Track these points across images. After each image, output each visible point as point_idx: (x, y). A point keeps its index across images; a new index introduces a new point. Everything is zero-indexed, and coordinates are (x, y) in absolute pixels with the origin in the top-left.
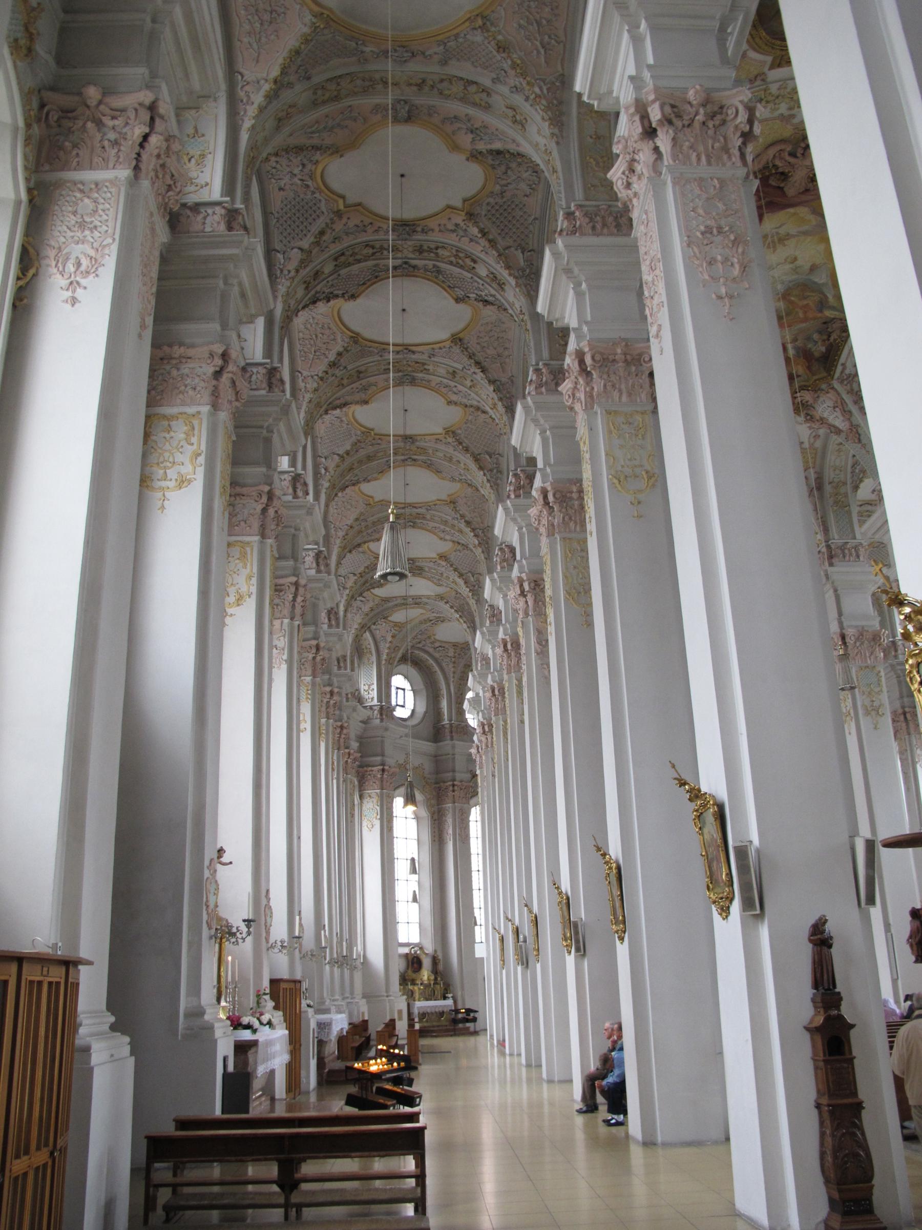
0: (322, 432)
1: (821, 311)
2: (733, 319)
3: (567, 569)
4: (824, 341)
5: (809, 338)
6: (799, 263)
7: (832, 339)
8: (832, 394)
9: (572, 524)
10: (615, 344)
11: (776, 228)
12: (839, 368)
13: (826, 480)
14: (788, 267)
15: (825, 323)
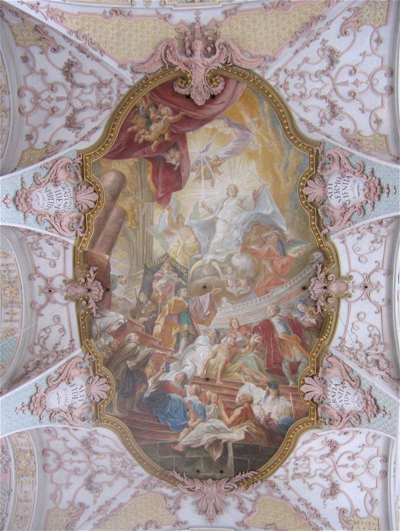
1: (284, 254)
5: (293, 308)
7: (319, 308)
11: (204, 151)
14: (233, 202)
15: (304, 288)
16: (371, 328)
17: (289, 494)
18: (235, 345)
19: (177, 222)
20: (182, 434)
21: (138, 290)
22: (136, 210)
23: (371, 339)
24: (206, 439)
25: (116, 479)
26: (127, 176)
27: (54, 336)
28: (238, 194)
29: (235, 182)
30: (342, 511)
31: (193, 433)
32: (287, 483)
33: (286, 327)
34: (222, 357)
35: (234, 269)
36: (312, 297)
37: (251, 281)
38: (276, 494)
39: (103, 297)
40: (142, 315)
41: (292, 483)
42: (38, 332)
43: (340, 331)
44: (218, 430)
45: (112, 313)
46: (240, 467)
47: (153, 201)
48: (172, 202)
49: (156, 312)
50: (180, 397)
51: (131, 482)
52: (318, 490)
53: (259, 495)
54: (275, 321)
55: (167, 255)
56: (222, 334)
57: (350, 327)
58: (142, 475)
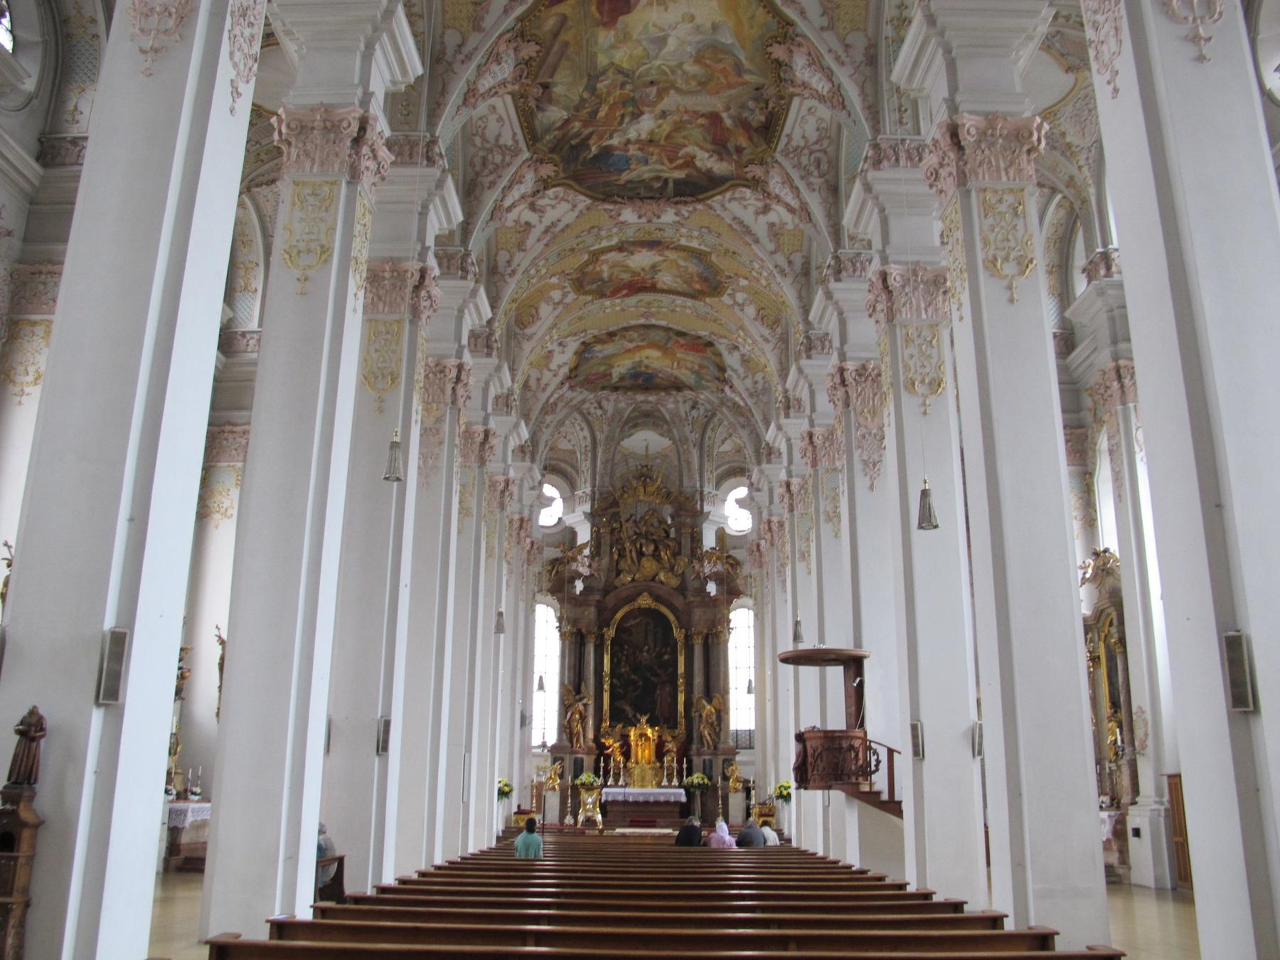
0: (269, 210)
1: (740, 75)
2: (150, 75)
3: (368, 352)
4: (762, 109)
5: (743, 106)
6: (698, 21)
8: (777, 169)
9: (381, 306)
10: (313, 110)
12: (784, 140)
13: (813, 264)
15: (757, 89)
16: (819, 122)
17: (723, 214)
18: (681, 121)
19: (625, 37)
20: (624, 174)
21: (581, 90)
22: (579, 38)
23: (818, 133)
24: (646, 176)
25: (559, 203)
26: (566, 12)
27: (492, 128)
28: (695, 21)
29: (692, 11)
30: (772, 225)
31: (635, 172)
32: (723, 206)
33: (734, 122)
34: (667, 127)
35: (684, 72)
36: (764, 96)
37: (703, 84)
38: (713, 212)
39: (543, 93)
40: (585, 108)
41: (727, 205)
42: (474, 122)
43: (787, 130)
44: (662, 171)
45: (555, 108)
46: (678, 193)
47: (598, 26)
48: (619, 25)
49: (601, 103)
50: (623, 153)
51: (575, 206)
52: (751, 210)
53: (695, 210)
54: (724, 115)
55: (612, 64)
56: (668, 113)
57: (799, 120)
58: (585, 201)
